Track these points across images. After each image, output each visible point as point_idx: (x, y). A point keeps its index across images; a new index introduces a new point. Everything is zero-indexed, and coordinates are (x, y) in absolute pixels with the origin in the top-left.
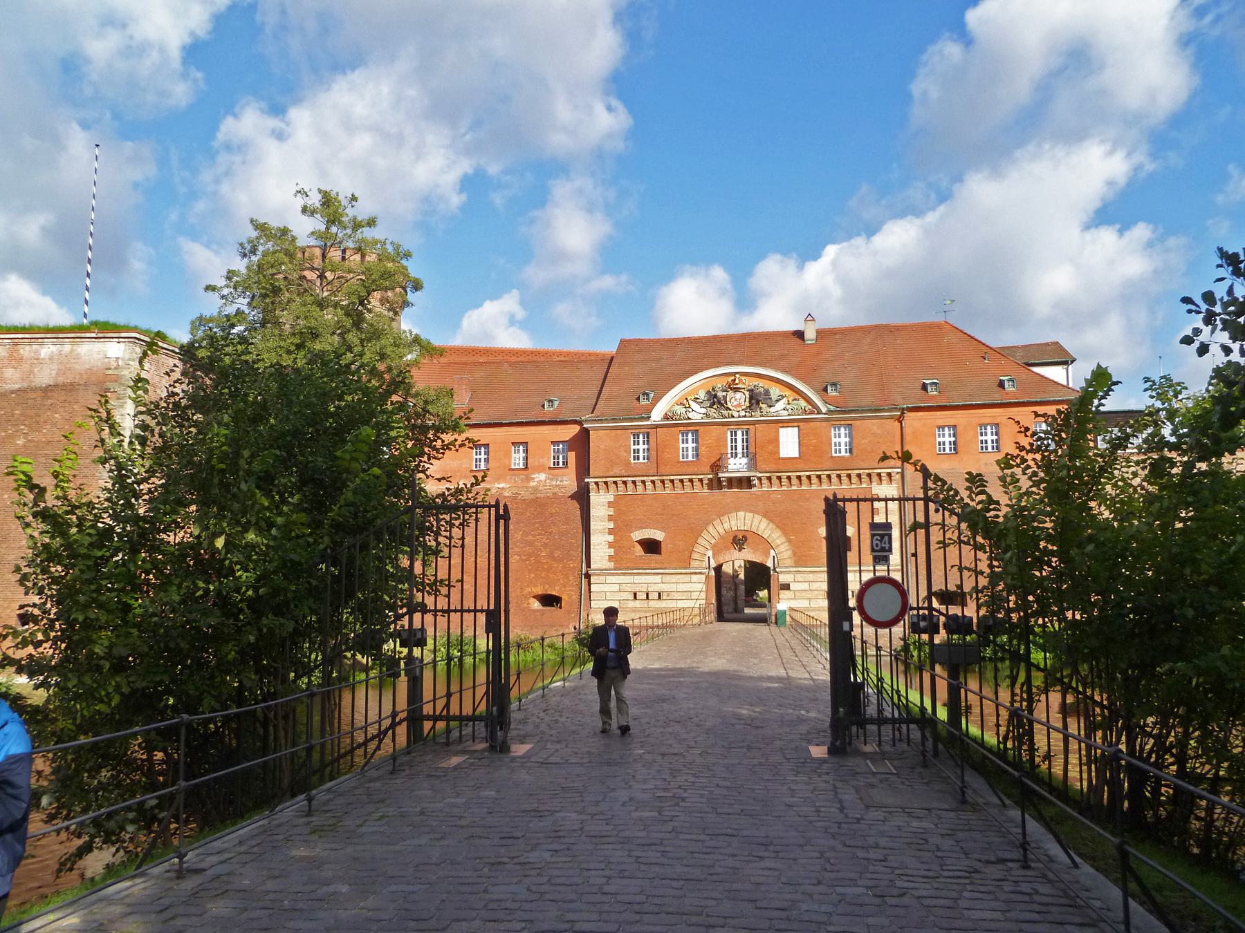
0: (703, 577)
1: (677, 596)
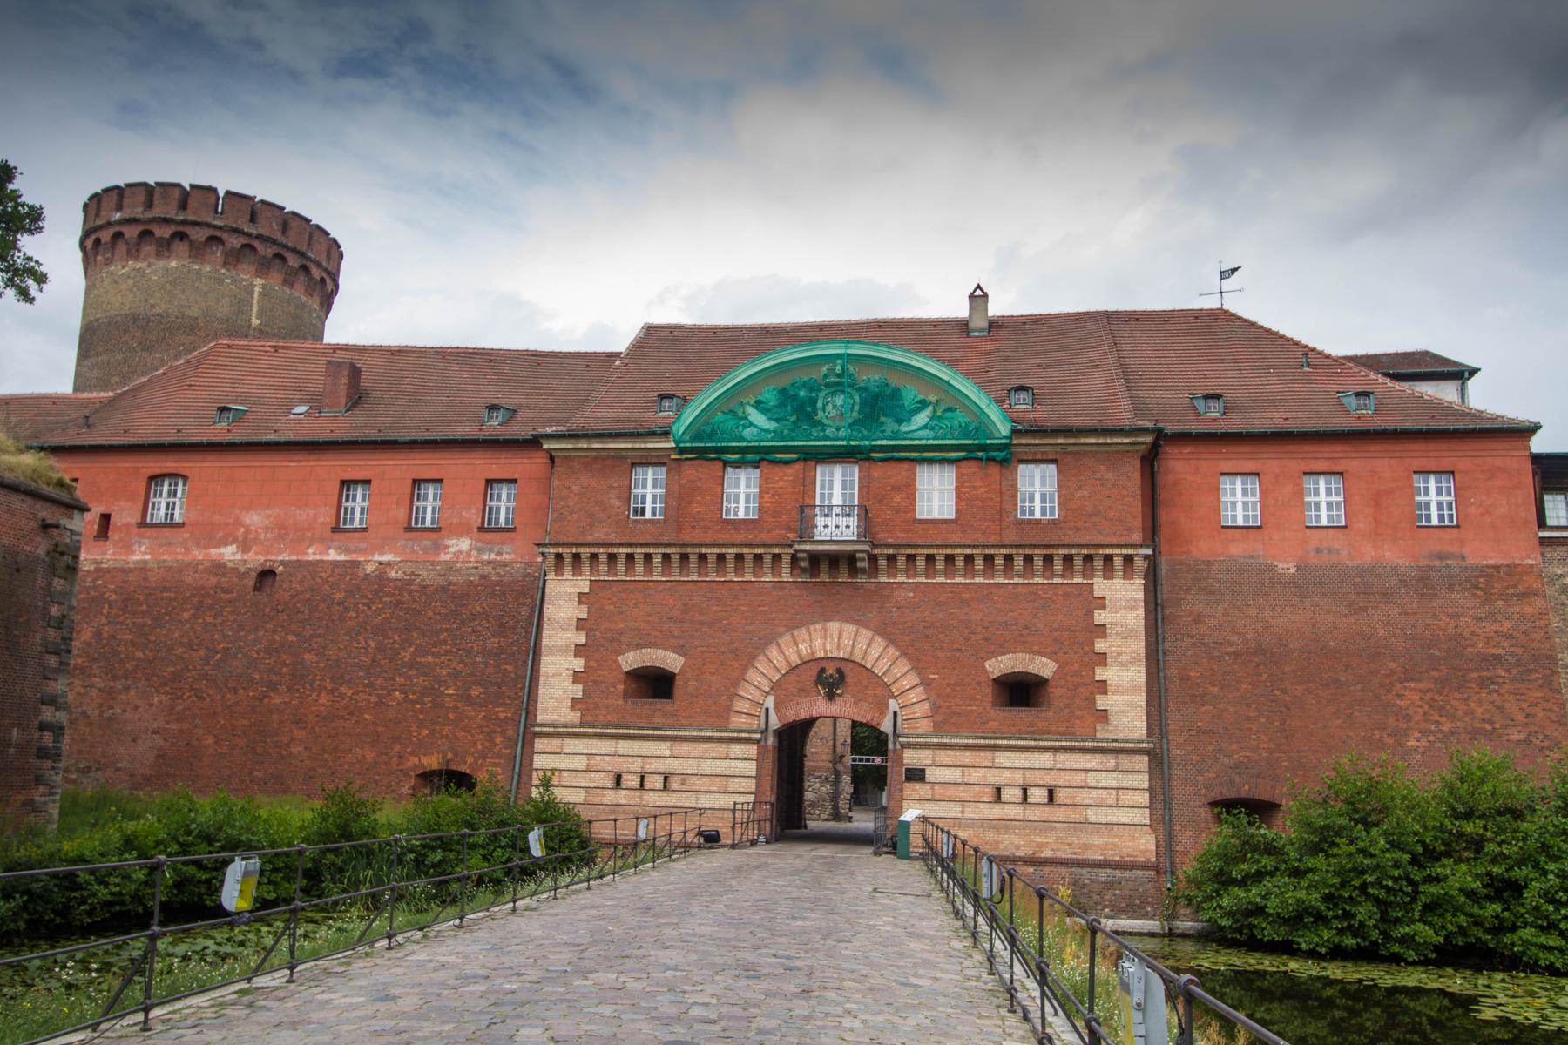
0: (753, 749)
1: (699, 783)
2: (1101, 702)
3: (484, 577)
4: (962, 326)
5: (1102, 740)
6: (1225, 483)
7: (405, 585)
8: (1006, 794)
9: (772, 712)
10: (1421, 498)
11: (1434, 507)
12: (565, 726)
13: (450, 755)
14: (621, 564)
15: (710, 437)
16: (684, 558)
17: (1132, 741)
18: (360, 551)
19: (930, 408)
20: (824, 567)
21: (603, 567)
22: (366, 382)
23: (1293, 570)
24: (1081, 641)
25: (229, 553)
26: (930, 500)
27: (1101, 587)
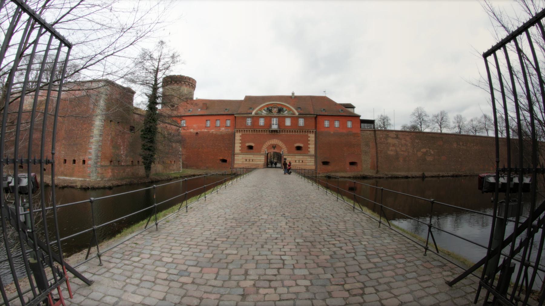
4: (291, 97)
7: (216, 134)
24: (307, 142)
25: (192, 130)
27: (309, 135)
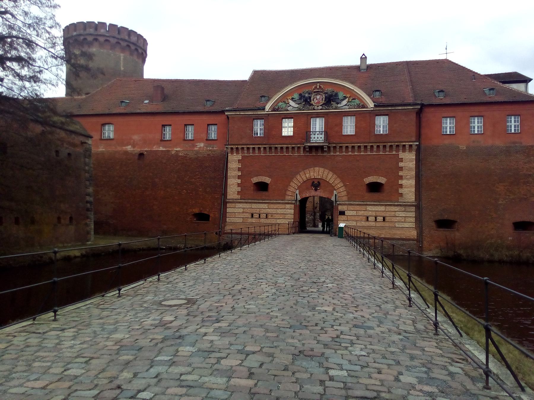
2: (401, 191)
3: (208, 155)
4: (358, 68)
5: (400, 202)
6: (444, 120)
7: (185, 157)
8: (370, 219)
9: (298, 195)
10: (509, 124)
11: (513, 127)
12: (236, 199)
13: (201, 209)
14: (251, 150)
15: (277, 110)
16: (270, 148)
17: (410, 202)
18: (170, 147)
19: (347, 99)
20: (314, 150)
21: (246, 152)
22: (166, 91)
23: (465, 148)
24: (395, 172)
25: (129, 148)
26: (347, 128)
27: (401, 155)
